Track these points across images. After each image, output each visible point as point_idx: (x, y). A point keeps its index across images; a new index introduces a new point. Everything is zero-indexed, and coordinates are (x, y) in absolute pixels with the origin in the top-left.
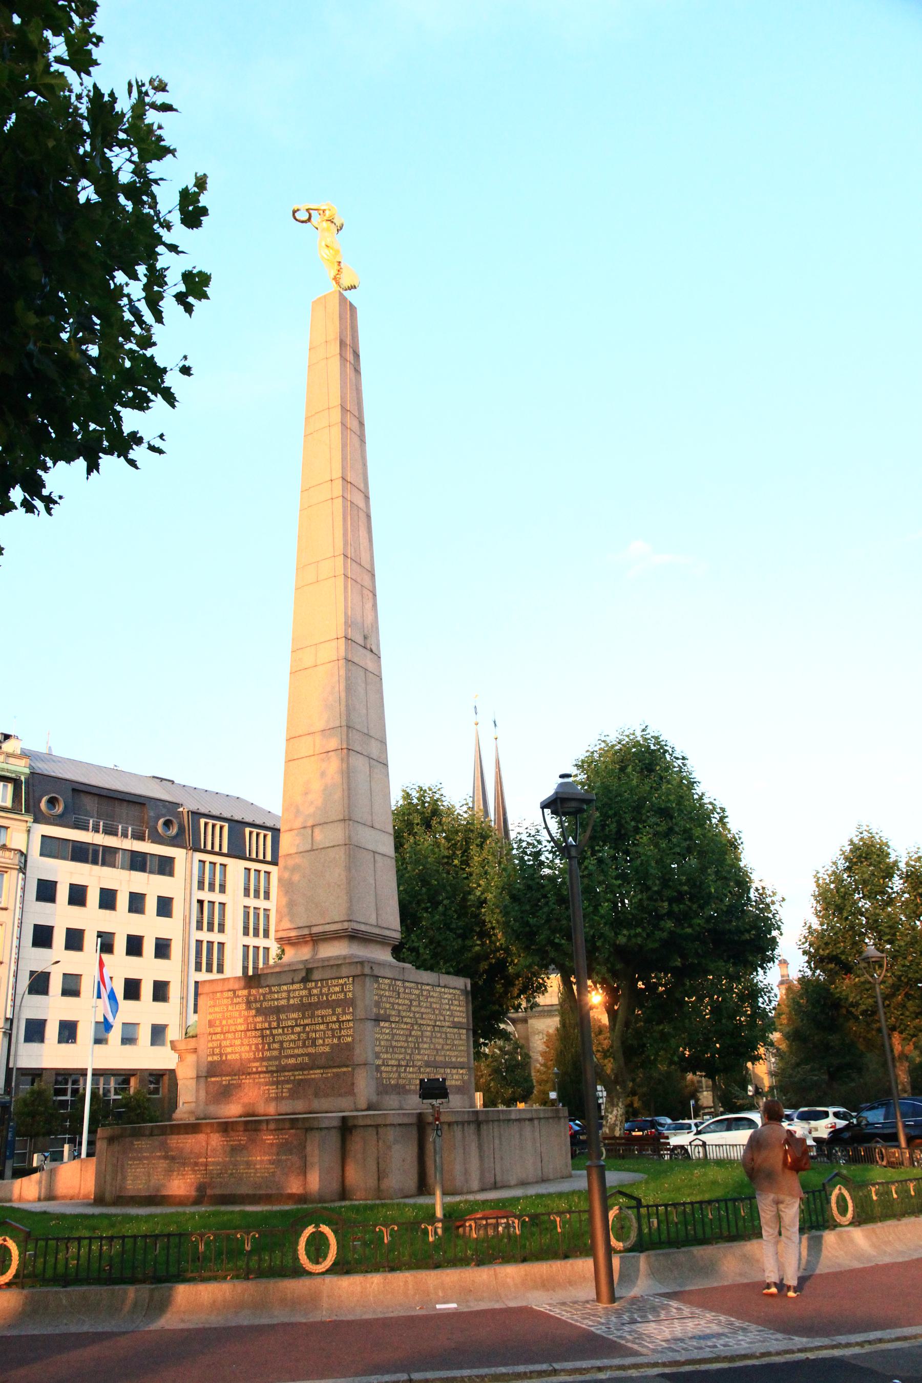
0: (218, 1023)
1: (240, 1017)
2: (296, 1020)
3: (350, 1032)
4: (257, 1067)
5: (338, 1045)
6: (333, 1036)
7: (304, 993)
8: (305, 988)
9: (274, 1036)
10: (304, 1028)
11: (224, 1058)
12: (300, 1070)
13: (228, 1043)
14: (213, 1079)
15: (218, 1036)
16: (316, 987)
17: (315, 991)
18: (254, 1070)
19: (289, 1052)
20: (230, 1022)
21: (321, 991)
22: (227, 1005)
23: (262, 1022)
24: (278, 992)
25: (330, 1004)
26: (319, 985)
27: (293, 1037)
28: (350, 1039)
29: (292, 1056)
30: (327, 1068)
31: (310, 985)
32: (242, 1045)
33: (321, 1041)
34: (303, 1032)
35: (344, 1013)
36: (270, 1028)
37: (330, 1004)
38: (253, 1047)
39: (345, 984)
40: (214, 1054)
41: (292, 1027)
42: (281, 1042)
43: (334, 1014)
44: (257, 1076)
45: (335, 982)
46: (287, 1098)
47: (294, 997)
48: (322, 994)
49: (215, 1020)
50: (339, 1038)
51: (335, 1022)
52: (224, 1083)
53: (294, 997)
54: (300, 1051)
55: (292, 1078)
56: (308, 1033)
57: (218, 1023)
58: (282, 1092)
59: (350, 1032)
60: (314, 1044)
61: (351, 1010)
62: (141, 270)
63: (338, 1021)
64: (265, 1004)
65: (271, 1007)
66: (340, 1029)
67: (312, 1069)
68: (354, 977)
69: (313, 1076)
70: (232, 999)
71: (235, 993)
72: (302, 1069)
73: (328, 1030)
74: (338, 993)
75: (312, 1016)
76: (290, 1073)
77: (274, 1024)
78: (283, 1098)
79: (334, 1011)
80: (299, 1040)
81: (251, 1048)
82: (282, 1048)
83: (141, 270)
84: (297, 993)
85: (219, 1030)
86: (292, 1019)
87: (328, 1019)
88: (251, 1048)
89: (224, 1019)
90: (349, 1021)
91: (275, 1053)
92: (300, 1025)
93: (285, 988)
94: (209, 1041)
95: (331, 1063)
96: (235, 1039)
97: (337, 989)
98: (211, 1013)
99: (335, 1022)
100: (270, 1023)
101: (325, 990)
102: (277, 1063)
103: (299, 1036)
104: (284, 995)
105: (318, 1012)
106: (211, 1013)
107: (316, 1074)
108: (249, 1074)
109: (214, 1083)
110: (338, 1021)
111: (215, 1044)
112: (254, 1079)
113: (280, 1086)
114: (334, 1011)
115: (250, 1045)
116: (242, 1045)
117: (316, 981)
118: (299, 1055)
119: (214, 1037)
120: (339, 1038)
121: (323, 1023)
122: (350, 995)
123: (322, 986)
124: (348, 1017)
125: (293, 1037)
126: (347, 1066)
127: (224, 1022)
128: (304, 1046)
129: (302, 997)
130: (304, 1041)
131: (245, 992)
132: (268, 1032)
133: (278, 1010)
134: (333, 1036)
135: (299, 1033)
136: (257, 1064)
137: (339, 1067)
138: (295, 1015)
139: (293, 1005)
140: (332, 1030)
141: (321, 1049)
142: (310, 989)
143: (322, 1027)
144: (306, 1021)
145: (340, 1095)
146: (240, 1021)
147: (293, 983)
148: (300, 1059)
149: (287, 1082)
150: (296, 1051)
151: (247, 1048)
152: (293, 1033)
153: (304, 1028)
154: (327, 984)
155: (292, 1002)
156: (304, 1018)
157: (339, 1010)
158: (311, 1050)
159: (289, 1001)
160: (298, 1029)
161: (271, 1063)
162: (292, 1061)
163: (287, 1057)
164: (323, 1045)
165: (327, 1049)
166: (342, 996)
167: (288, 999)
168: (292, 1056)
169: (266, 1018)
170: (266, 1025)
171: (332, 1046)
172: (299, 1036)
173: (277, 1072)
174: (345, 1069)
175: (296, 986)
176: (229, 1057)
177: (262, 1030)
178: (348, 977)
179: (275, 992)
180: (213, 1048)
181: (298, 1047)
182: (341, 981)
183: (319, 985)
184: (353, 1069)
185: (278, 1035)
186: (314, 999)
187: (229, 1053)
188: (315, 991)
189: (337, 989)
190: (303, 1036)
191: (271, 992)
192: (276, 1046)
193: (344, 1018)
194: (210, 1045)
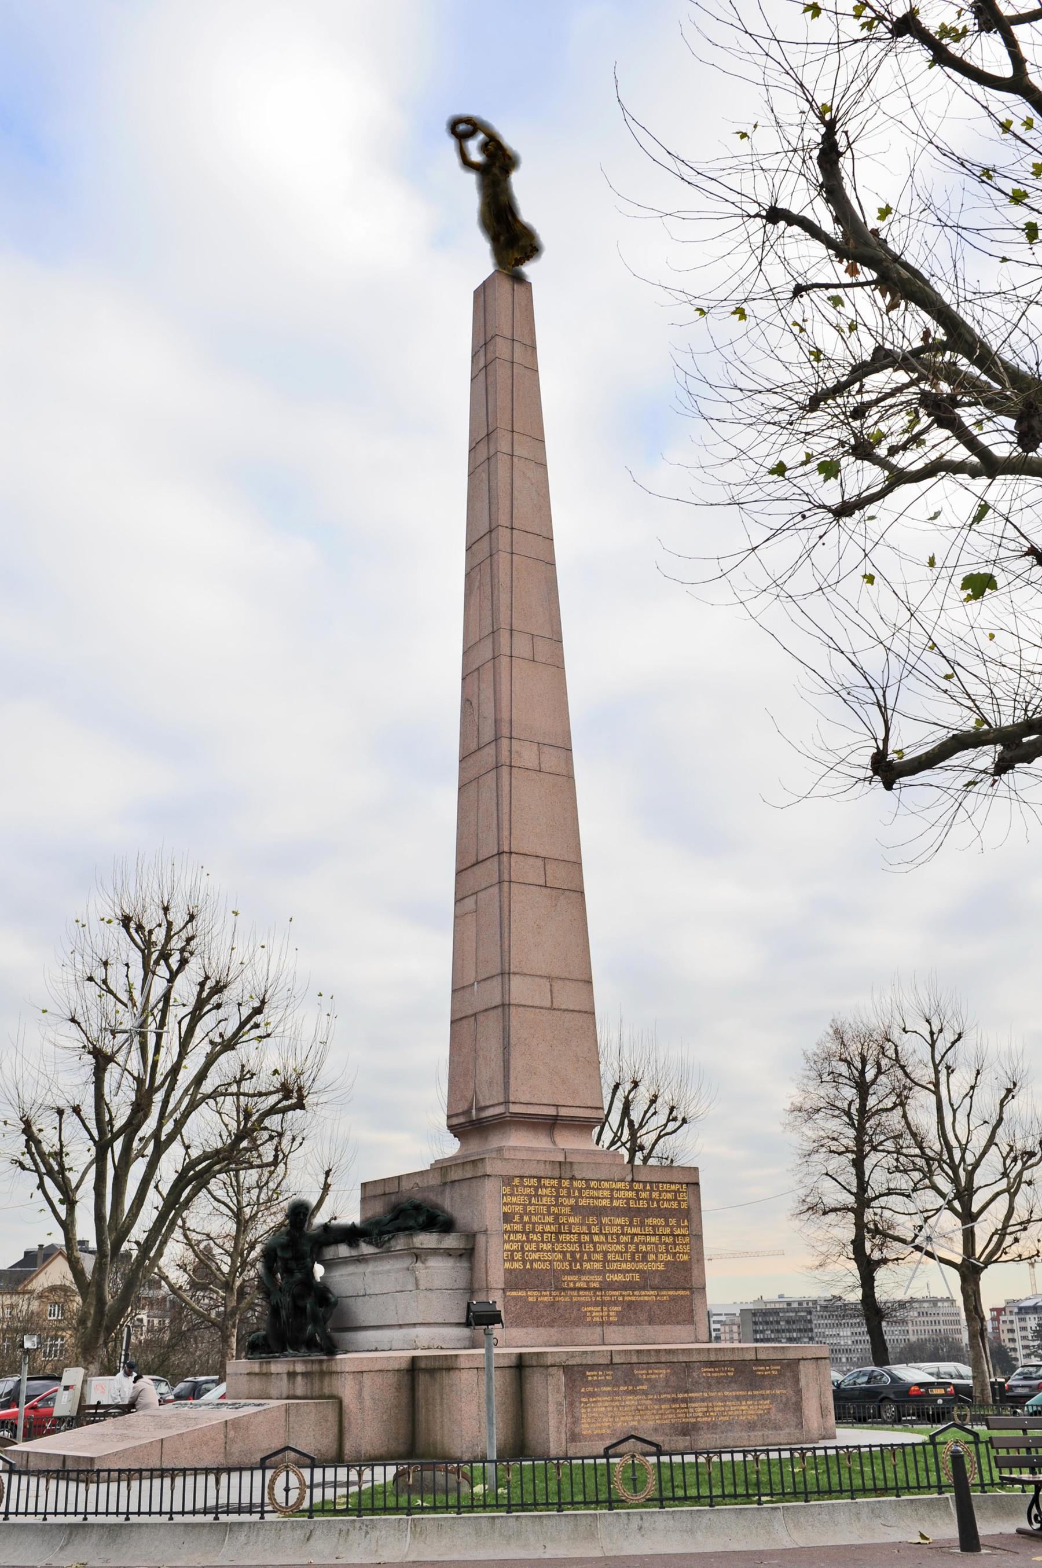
0: (517, 1218)
1: (549, 1214)
2: (622, 1227)
3: (687, 1249)
4: (575, 1283)
5: (673, 1263)
7: (631, 1194)
9: (595, 1244)
10: (632, 1239)
11: (528, 1266)
12: (630, 1289)
13: (534, 1245)
14: (514, 1293)
15: (519, 1237)
16: (645, 1190)
17: (644, 1195)
18: (571, 1285)
19: (614, 1266)
20: (534, 1219)
21: (651, 1195)
22: (530, 1197)
23: (579, 1224)
24: (598, 1189)
25: (660, 1213)
26: (648, 1187)
27: (619, 1248)
28: (686, 1258)
29: (619, 1271)
30: (661, 1289)
33: (652, 1257)
34: (632, 1243)
35: (679, 1226)
36: (590, 1234)
37: (660, 1213)
38: (568, 1255)
39: (678, 1191)
40: (512, 1260)
41: (618, 1235)
42: (605, 1253)
43: (667, 1225)
44: (575, 1293)
45: (666, 1187)
46: (615, 1324)
47: (618, 1198)
48: (653, 1200)
49: (514, 1214)
50: (674, 1255)
51: (668, 1235)
52: (530, 1299)
53: (618, 1198)
54: (629, 1266)
55: (621, 1299)
56: (637, 1245)
57: (517, 1218)
58: (609, 1316)
59: (687, 1249)
60: (644, 1259)
61: (686, 1223)
62: (930, 341)
64: (582, 1202)
65: (589, 1206)
66: (675, 1244)
67: (644, 1288)
68: (687, 1184)
69: (646, 1298)
70: (536, 1189)
71: (539, 1182)
72: (633, 1289)
73: (661, 1244)
74: (670, 1200)
75: (642, 1225)
76: (617, 1293)
77: (595, 1229)
78: (610, 1323)
79: (667, 1221)
80: (626, 1252)
81: (565, 1256)
82: (605, 1260)
83: (930, 341)
84: (622, 1192)
85: (519, 1227)
86: (617, 1225)
87: (661, 1231)
88: (565, 1256)
89: (526, 1213)
90: (684, 1235)
91: (598, 1266)
92: (627, 1234)
93: (606, 1185)
94: (505, 1242)
95: (666, 1284)
96: (543, 1241)
97: (669, 1196)
98: (505, 1204)
99: (668, 1235)
100: (589, 1227)
101: (655, 1195)
102: (600, 1278)
103: (626, 1247)
105: (649, 1221)
106: (505, 1204)
107: (649, 1296)
108: (564, 1289)
109: (514, 1298)
111: (515, 1247)
112: (571, 1297)
113: (605, 1309)
114: (667, 1221)
115: (564, 1253)
117: (644, 1183)
118: (628, 1271)
121: (655, 1235)
122: (684, 1206)
123: (651, 1190)
124: (684, 1231)
125: (619, 1248)
126: (684, 1289)
127: (526, 1219)
128: (633, 1260)
129: (628, 1199)
130: (633, 1254)
135: (626, 1244)
136: (575, 1278)
137: (676, 1289)
138: (618, 1221)
139: (617, 1208)
140: (667, 1244)
141: (654, 1267)
142: (637, 1191)
143: (654, 1239)
144: (634, 1230)
145: (678, 1323)
146: (551, 1219)
148: (628, 1277)
149: (615, 1303)
150: (624, 1266)
151: (560, 1256)
152: (618, 1243)
153: (632, 1239)
154: (658, 1187)
155: (615, 1203)
156: (631, 1225)
157: (673, 1222)
158: (641, 1266)
159: (612, 1202)
160: (624, 1239)
161: (592, 1278)
162: (618, 1278)
163: (612, 1272)
164: (656, 1262)
165: (661, 1267)
166: (675, 1205)
167: (612, 1199)
169: (584, 1218)
170: (585, 1229)
171: (667, 1263)
172: (626, 1247)
173: (601, 1289)
174: (682, 1293)
175: (620, 1185)
176: (535, 1266)
177: (579, 1234)
178: (681, 1184)
179: (593, 1189)
180: (512, 1252)
181: (626, 1261)
182: (673, 1187)
183: (648, 1187)
184: (692, 1293)
185: (600, 1243)
186: (643, 1204)
187: (536, 1261)
188: (644, 1195)
189: (669, 1196)
191: (588, 1187)
192: (599, 1257)
193: (678, 1232)
194: (507, 1246)
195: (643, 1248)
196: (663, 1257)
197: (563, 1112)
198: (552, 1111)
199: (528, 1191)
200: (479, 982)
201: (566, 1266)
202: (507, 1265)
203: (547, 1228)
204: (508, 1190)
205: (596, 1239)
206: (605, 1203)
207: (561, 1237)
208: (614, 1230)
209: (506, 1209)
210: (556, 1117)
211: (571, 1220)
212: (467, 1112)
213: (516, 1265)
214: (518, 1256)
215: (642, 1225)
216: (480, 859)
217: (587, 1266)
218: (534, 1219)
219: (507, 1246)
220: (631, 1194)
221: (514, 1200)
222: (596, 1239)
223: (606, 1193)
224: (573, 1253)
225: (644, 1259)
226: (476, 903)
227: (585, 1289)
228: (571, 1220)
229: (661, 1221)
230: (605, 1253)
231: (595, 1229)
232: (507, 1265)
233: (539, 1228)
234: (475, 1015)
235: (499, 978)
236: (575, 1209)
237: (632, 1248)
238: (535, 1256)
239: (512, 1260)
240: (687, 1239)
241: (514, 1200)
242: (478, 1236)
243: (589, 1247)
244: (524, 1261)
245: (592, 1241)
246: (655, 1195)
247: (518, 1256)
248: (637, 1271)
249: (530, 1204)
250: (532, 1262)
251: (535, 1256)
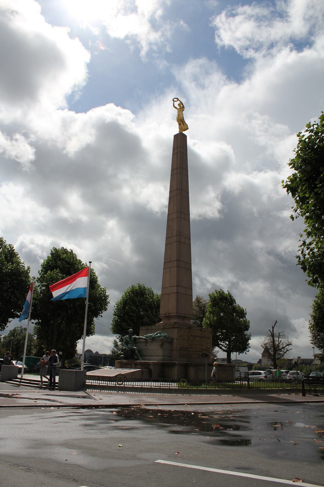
0: (182, 337)
8: (201, 332)
17: (203, 333)
27: (198, 344)
28: (209, 346)
29: (198, 348)
31: (202, 332)
42: (196, 344)
47: (199, 334)
64: (193, 334)
77: (195, 340)
85: (182, 338)
91: (195, 347)
97: (207, 334)
101: (205, 334)
104: (197, 333)
105: (204, 339)
117: (203, 331)
119: (181, 340)
123: (204, 333)
125: (198, 344)
127: (183, 337)
132: (193, 341)
138: (199, 338)
143: (204, 342)
144: (201, 340)
147: (198, 330)
150: (199, 347)
158: (202, 347)
162: (198, 349)
168: (198, 348)
181: (199, 346)
194: (180, 342)
195: (202, 344)
197: (186, 316)
198: (184, 315)
200: (170, 287)
202: (180, 346)
203: (187, 339)
204: (180, 331)
205: (195, 341)
206: (196, 335)
207: (189, 341)
208: (198, 340)
209: (180, 334)
210: (185, 317)
211: (191, 338)
212: (166, 314)
213: (181, 346)
216: (171, 261)
217: (193, 347)
218: (185, 337)
219: (180, 342)
220: (201, 333)
221: (181, 333)
222: (195, 341)
223: (197, 333)
225: (202, 346)
226: (170, 270)
227: (192, 351)
228: (191, 338)
229: (205, 339)
231: (195, 340)
232: (180, 346)
233: (185, 339)
234: (169, 294)
235: (176, 287)
237: (200, 344)
238: (185, 344)
239: (180, 345)
241: (181, 333)
242: (174, 340)
243: (193, 343)
246: (205, 334)
247: (181, 344)
248: (201, 348)
249: (184, 334)
250: (184, 345)
251: (185, 344)
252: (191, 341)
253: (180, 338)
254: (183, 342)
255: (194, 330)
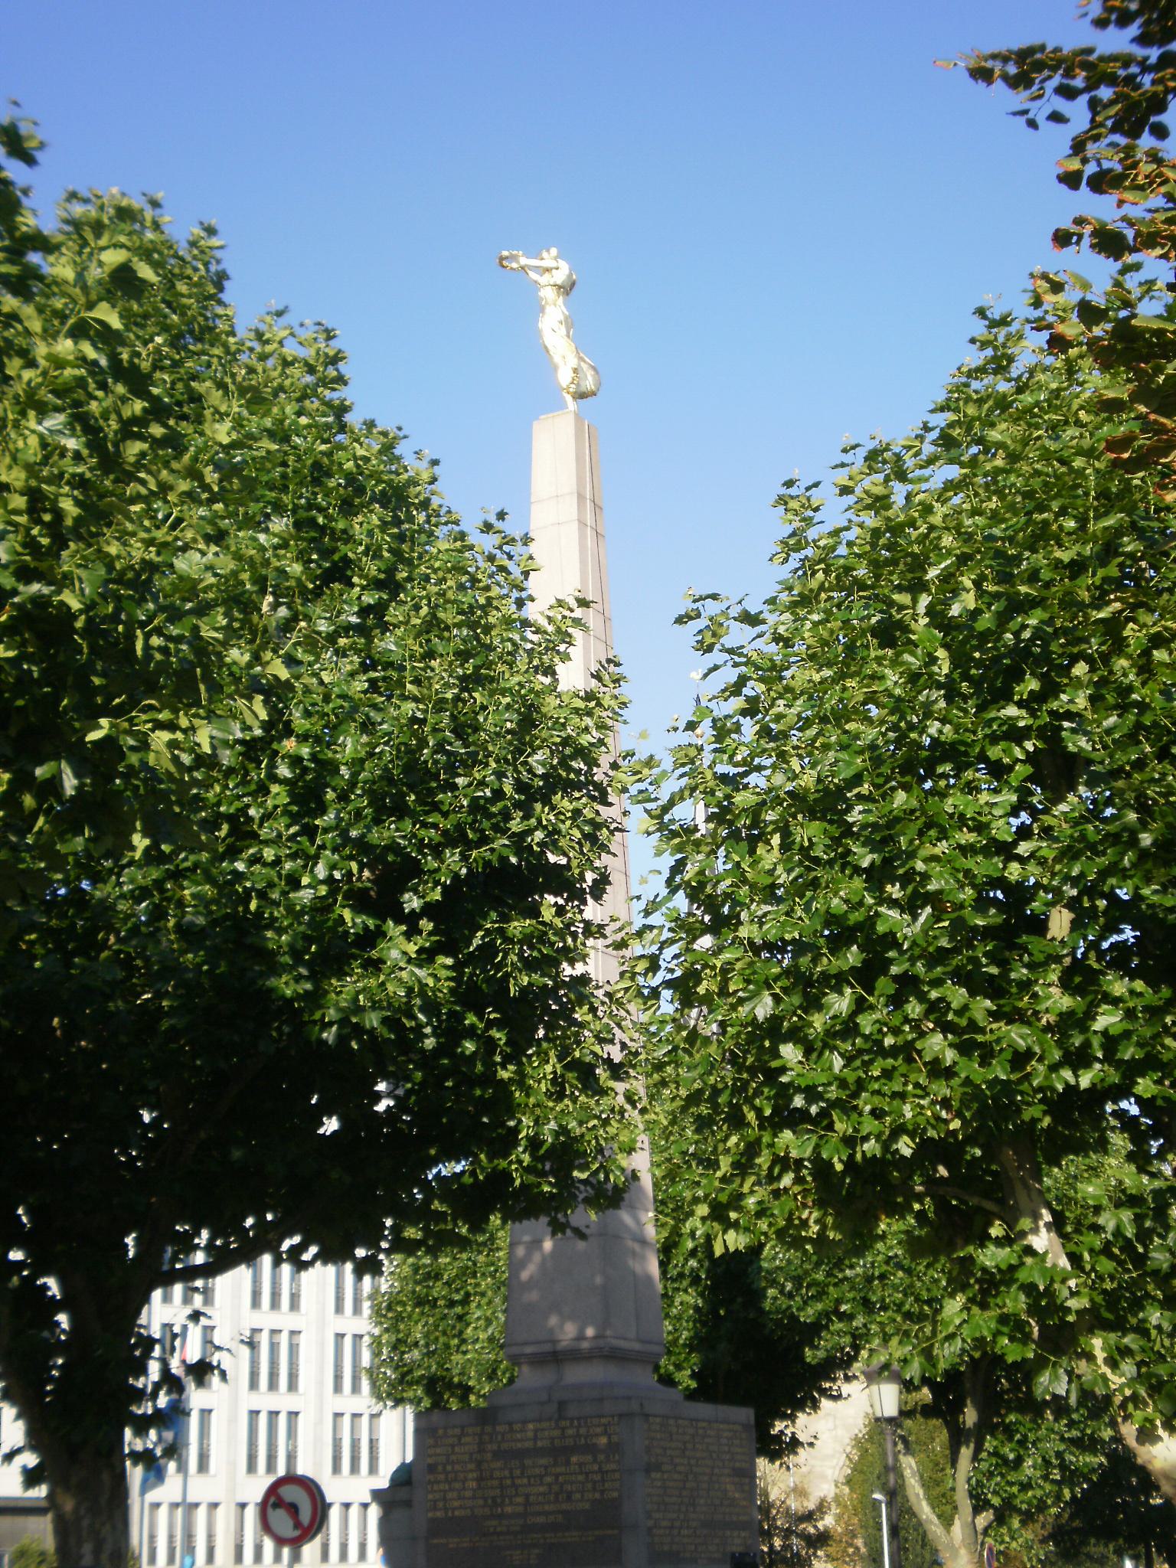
6: (594, 1489)
7: (556, 1433)
17: (570, 1432)
20: (457, 1467)
27: (541, 1489)
28: (615, 1494)
29: (539, 1514)
31: (563, 1423)
32: (474, 1498)
33: (578, 1496)
41: (541, 1477)
42: (527, 1496)
43: (595, 1460)
45: (595, 1421)
48: (578, 1436)
50: (602, 1492)
60: (569, 1498)
63: (600, 1471)
64: (505, 1446)
66: (603, 1481)
82: (527, 1503)
91: (520, 1509)
97: (599, 1430)
101: (583, 1431)
104: (530, 1434)
105: (574, 1459)
110: (600, 1471)
111: (437, 1496)
115: (485, 1499)
116: (474, 1498)
117: (572, 1419)
120: (602, 1492)
124: (613, 1466)
129: (552, 1439)
131: (478, 1429)
133: (521, 1454)
134: (594, 1489)
135: (550, 1485)
136: (494, 1523)
138: (543, 1461)
140: (595, 1482)
142: (563, 1429)
143: (581, 1478)
144: (559, 1470)
148: (551, 1518)
151: (481, 1502)
155: (539, 1444)
158: (565, 1506)
162: (541, 1520)
165: (587, 1506)
168: (539, 1514)
175: (545, 1425)
182: (604, 1421)
186: (569, 1442)
188: (570, 1432)
190: (556, 1488)
192: (520, 1500)
196: (590, 1496)
199: (450, 1441)
201: (487, 1511)
205: (518, 1482)
206: (529, 1444)
208: (537, 1471)
213: (439, 1514)
214: (441, 1504)
215: (568, 1463)
217: (509, 1509)
218: (457, 1467)
220: (556, 1433)
224: (494, 1499)
229: (589, 1458)
230: (527, 1496)
233: (461, 1476)
236: (497, 1454)
239: (435, 1508)
240: (617, 1475)
244: (446, 1509)
245: (513, 1485)
246: (583, 1431)
247: (441, 1504)
251: (456, 1504)
252: (495, 1483)
253: (431, 1477)
254: (450, 1495)
255: (510, 1424)
